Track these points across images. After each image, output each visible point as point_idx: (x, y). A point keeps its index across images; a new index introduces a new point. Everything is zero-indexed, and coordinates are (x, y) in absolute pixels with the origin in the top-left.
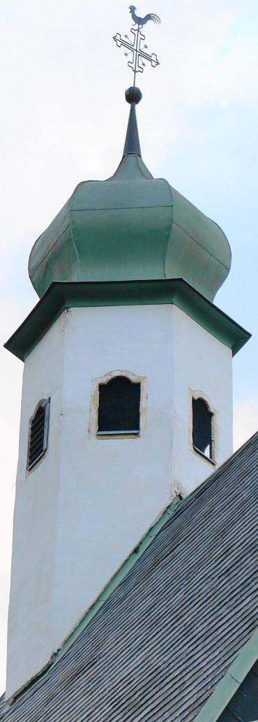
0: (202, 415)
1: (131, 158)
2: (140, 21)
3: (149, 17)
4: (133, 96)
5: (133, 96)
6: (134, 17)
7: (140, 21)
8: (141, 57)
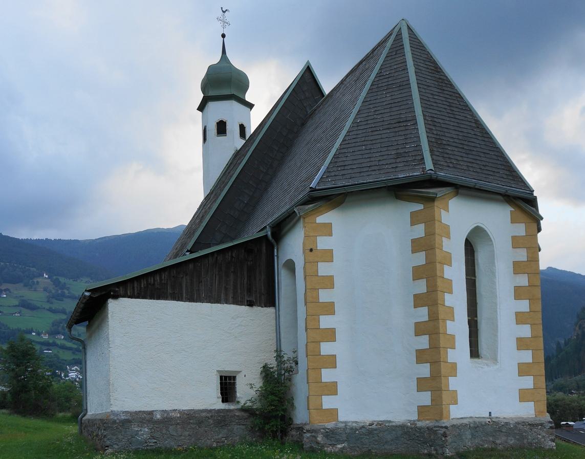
0: (242, 128)
1: (223, 55)
2: (224, 12)
3: (226, 10)
4: (223, 36)
5: (223, 36)
6: (222, 11)
7: (224, 12)
8: (225, 23)
